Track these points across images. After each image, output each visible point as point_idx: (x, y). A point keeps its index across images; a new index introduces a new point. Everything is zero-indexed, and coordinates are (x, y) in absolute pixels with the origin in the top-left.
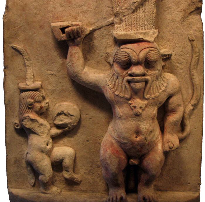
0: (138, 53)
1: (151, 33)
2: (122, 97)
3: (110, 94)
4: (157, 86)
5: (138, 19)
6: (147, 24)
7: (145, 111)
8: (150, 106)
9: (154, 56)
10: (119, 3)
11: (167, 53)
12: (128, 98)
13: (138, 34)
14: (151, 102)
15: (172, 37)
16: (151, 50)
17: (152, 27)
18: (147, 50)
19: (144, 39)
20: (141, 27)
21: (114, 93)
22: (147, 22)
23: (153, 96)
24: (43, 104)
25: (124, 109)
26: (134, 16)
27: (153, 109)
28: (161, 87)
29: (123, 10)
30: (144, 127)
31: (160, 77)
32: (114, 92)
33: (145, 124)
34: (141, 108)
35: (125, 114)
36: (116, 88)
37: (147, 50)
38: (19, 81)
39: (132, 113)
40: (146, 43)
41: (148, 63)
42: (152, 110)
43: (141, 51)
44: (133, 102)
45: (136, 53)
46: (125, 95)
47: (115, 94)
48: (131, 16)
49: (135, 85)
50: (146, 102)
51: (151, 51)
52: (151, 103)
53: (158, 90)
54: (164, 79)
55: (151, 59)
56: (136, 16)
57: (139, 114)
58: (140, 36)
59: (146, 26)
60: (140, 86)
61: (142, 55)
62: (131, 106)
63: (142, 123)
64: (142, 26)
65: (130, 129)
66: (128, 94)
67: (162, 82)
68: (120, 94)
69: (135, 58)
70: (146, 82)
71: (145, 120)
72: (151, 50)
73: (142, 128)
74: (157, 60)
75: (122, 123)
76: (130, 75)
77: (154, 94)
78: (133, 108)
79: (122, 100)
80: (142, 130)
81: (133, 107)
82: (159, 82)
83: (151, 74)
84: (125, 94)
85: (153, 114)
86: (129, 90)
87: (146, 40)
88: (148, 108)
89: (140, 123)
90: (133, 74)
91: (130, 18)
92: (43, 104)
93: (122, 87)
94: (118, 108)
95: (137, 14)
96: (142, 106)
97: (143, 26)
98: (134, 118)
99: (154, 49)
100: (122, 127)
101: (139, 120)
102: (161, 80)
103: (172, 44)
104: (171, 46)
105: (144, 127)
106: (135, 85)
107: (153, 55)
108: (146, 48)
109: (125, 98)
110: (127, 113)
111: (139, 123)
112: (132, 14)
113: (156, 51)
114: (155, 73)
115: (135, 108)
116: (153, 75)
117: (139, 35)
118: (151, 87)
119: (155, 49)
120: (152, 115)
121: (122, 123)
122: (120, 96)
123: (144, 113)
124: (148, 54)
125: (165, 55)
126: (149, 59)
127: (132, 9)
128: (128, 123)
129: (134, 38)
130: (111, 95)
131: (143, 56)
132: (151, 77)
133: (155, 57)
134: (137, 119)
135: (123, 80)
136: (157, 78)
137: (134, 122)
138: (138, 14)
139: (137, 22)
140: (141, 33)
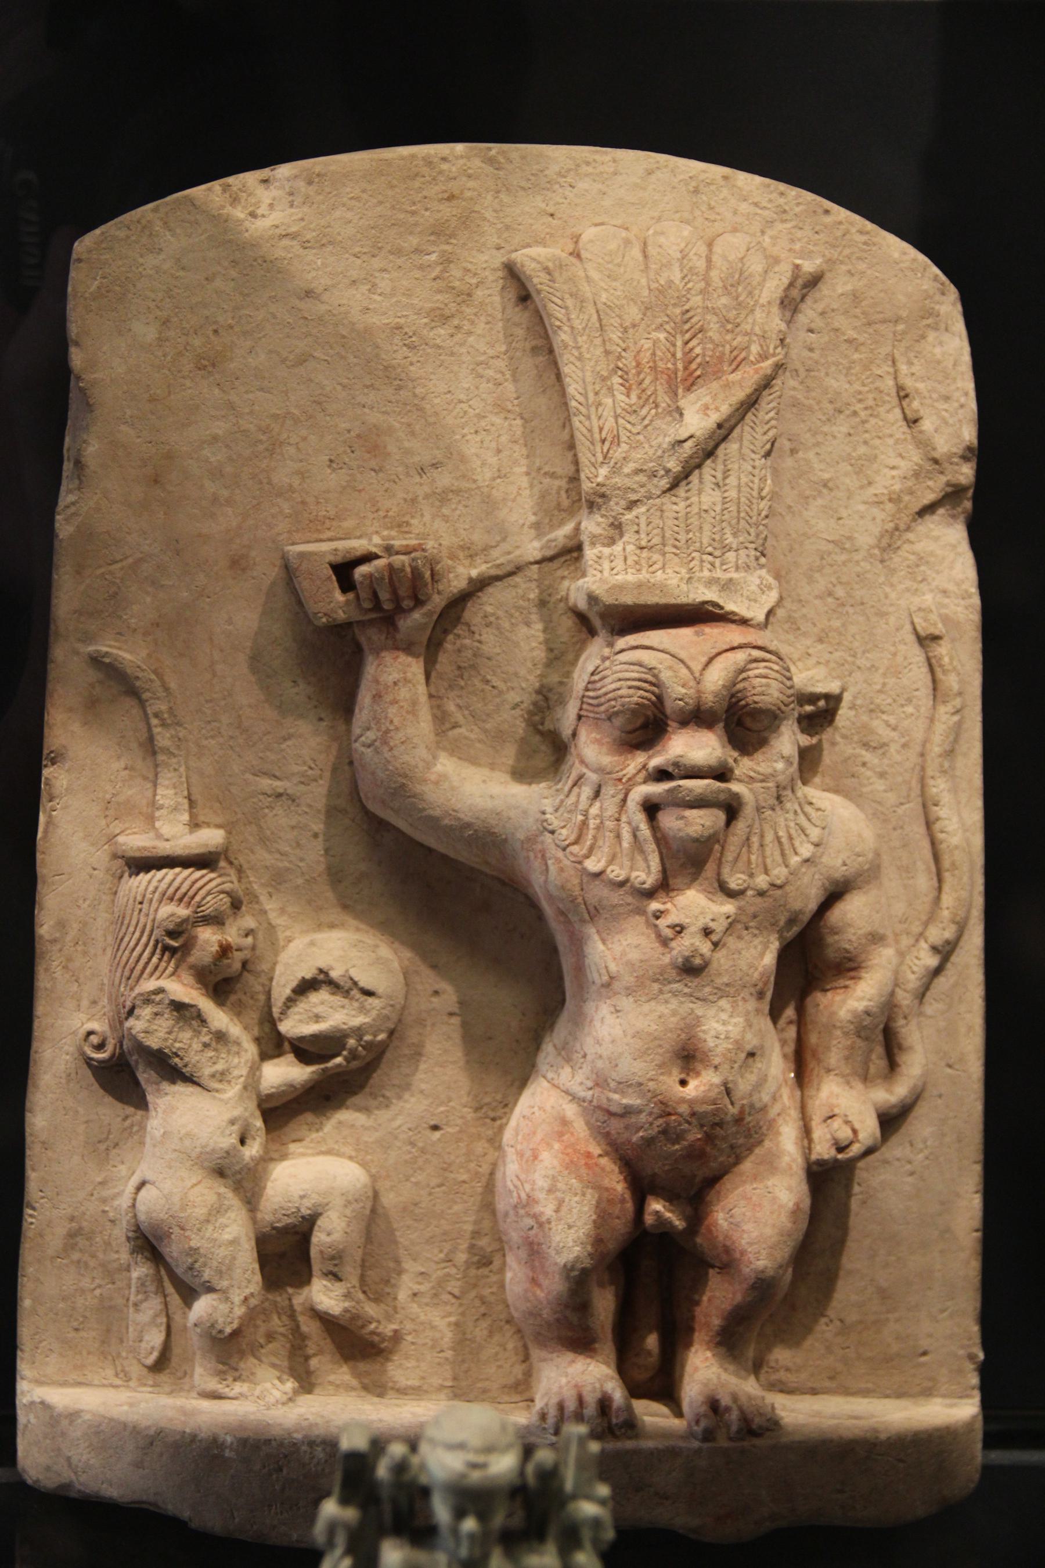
0: (697, 667)
1: (753, 588)
2: (622, 884)
3: (562, 870)
4: (781, 834)
5: (694, 521)
6: (734, 546)
7: (724, 952)
8: (747, 929)
9: (768, 685)
10: (607, 445)
11: (820, 689)
12: (646, 886)
13: (696, 585)
14: (751, 910)
15: (836, 623)
16: (756, 660)
17: (757, 559)
18: (741, 656)
19: (722, 608)
20: (705, 557)
21: (579, 866)
22: (735, 535)
23: (761, 881)
24: (232, 934)
25: (629, 941)
26: (676, 506)
27: (760, 947)
28: (797, 843)
29: (628, 475)
30: (720, 1028)
31: (789, 792)
32: (580, 863)
33: (724, 1016)
34: (707, 932)
35: (630, 964)
36: (588, 843)
37: (741, 656)
38: (116, 827)
39: (667, 959)
40: (733, 626)
41: (740, 723)
42: (755, 947)
43: (711, 660)
44: (669, 906)
45: (688, 667)
46: (634, 874)
47: (585, 869)
48: (664, 508)
49: (683, 818)
50: (729, 907)
51: (754, 665)
52: (755, 917)
53: (783, 854)
54: (808, 809)
55: (756, 698)
56: (682, 505)
57: (698, 961)
58: (706, 591)
59: (731, 556)
60: (708, 823)
61: (716, 678)
62: (662, 923)
63: (712, 1012)
64: (710, 554)
65: (655, 1038)
66: (649, 867)
67: (802, 819)
68: (609, 870)
69: (684, 691)
70: (732, 809)
71: (722, 992)
72: (756, 660)
73: (713, 1033)
74: (783, 708)
75: (618, 1011)
76: (662, 775)
77: (766, 872)
78: (669, 933)
79: (616, 897)
80: (711, 1043)
81: (672, 927)
82: (786, 820)
83: (752, 774)
84: (632, 869)
85: (760, 969)
86: (651, 847)
87: (733, 613)
88: (740, 937)
89: (699, 1009)
90: (676, 764)
91: (658, 513)
92: (232, 934)
93: (618, 836)
94: (596, 937)
95: (687, 499)
96: (712, 925)
97: (717, 553)
98: (675, 986)
99: (768, 656)
100: (618, 1031)
101: (699, 995)
102: (796, 812)
103: (837, 654)
104: (832, 665)
105: (720, 1028)
106: (683, 818)
107: (764, 681)
108: (733, 649)
109: (632, 887)
110: (641, 961)
111: (699, 1012)
112: (666, 499)
113: (776, 667)
114: (770, 771)
115: (680, 932)
116: (762, 781)
117: (702, 589)
118: (755, 839)
119: (774, 658)
120: (756, 975)
121: (618, 1011)
122: (612, 876)
123: (721, 960)
124: (744, 675)
125: (813, 698)
126: (750, 700)
127: (668, 471)
128: (646, 1008)
129: (679, 601)
130: (564, 875)
131: (721, 683)
132: (751, 790)
133: (776, 694)
134: (686, 990)
135: (624, 800)
136: (778, 798)
137: (674, 1004)
138: (694, 499)
139: (688, 532)
140: (710, 582)
